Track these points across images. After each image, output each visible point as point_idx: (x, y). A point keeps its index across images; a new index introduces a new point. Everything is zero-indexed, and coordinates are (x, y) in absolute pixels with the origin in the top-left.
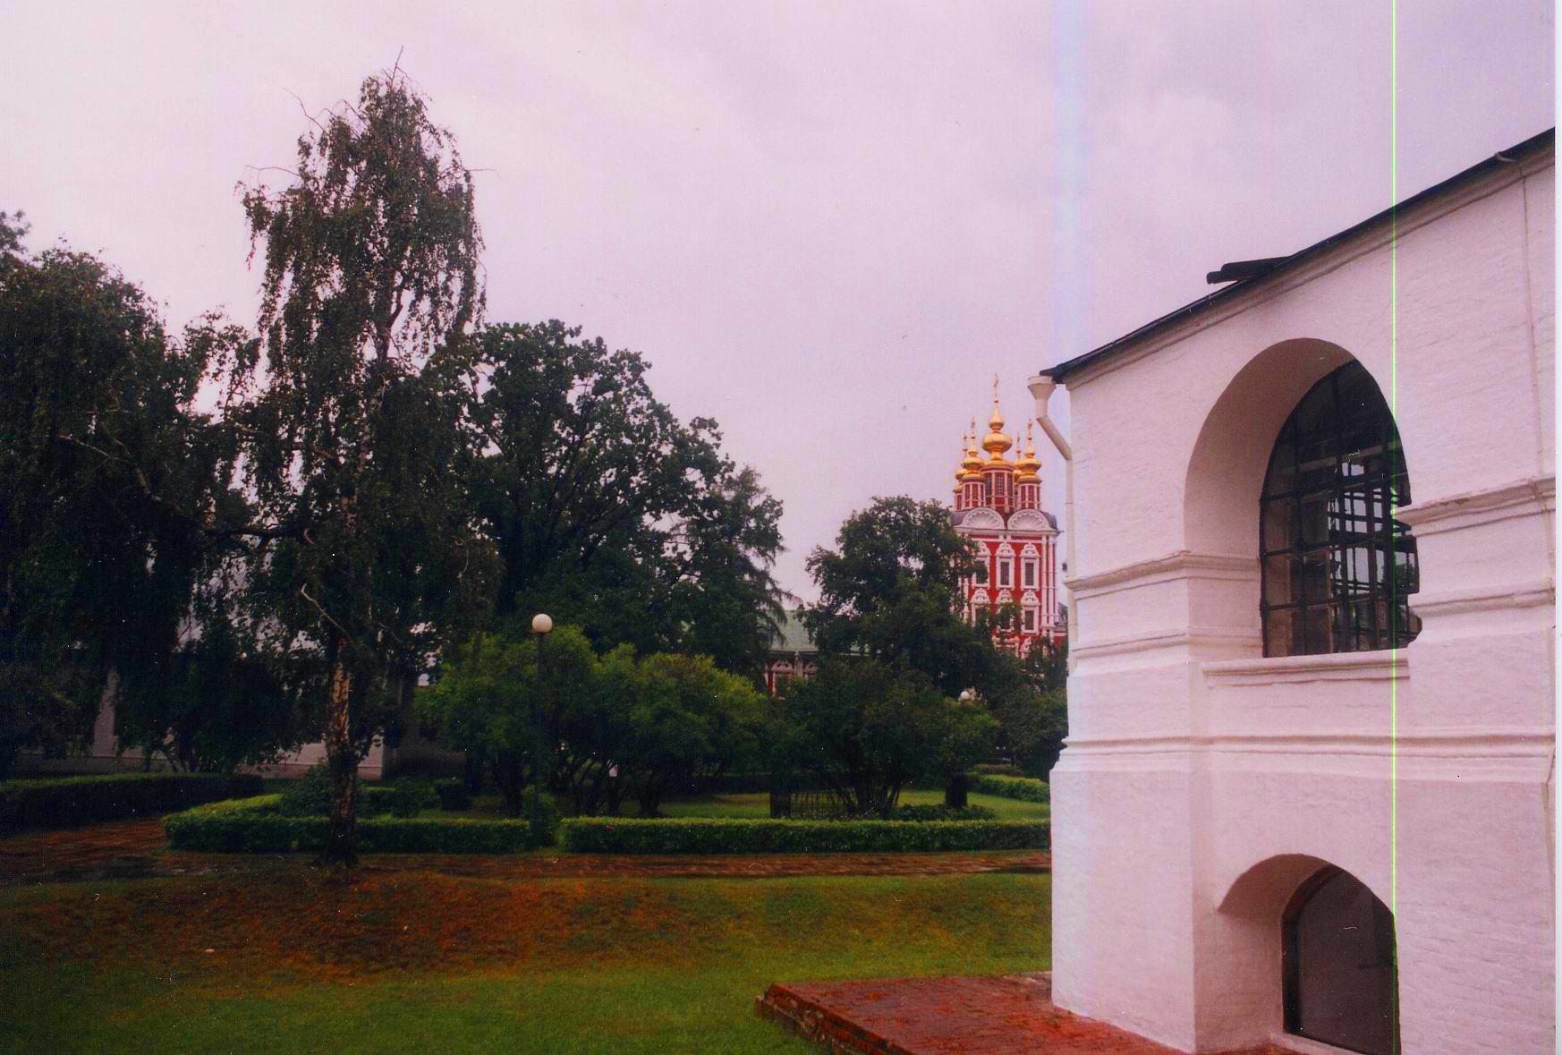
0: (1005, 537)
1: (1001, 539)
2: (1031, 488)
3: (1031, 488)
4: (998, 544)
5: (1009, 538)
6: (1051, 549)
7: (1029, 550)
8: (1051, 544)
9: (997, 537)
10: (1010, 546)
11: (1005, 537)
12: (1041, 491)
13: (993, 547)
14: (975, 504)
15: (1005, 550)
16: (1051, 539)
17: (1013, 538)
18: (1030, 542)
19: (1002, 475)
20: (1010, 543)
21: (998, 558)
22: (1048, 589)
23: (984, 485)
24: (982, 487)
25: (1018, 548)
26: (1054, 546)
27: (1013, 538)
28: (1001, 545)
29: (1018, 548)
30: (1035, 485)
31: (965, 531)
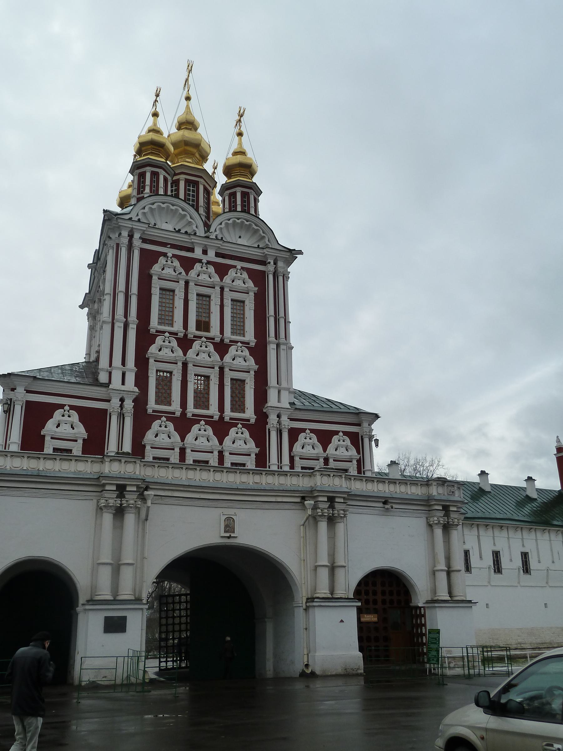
0: (205, 252)
1: (198, 253)
2: (245, 196)
5: (211, 256)
6: (281, 279)
8: (280, 270)
9: (192, 250)
10: (211, 269)
11: (205, 252)
16: (280, 264)
22: (278, 346)
23: (169, 178)
24: (166, 179)
26: (286, 277)
27: (218, 255)
31: (137, 225)
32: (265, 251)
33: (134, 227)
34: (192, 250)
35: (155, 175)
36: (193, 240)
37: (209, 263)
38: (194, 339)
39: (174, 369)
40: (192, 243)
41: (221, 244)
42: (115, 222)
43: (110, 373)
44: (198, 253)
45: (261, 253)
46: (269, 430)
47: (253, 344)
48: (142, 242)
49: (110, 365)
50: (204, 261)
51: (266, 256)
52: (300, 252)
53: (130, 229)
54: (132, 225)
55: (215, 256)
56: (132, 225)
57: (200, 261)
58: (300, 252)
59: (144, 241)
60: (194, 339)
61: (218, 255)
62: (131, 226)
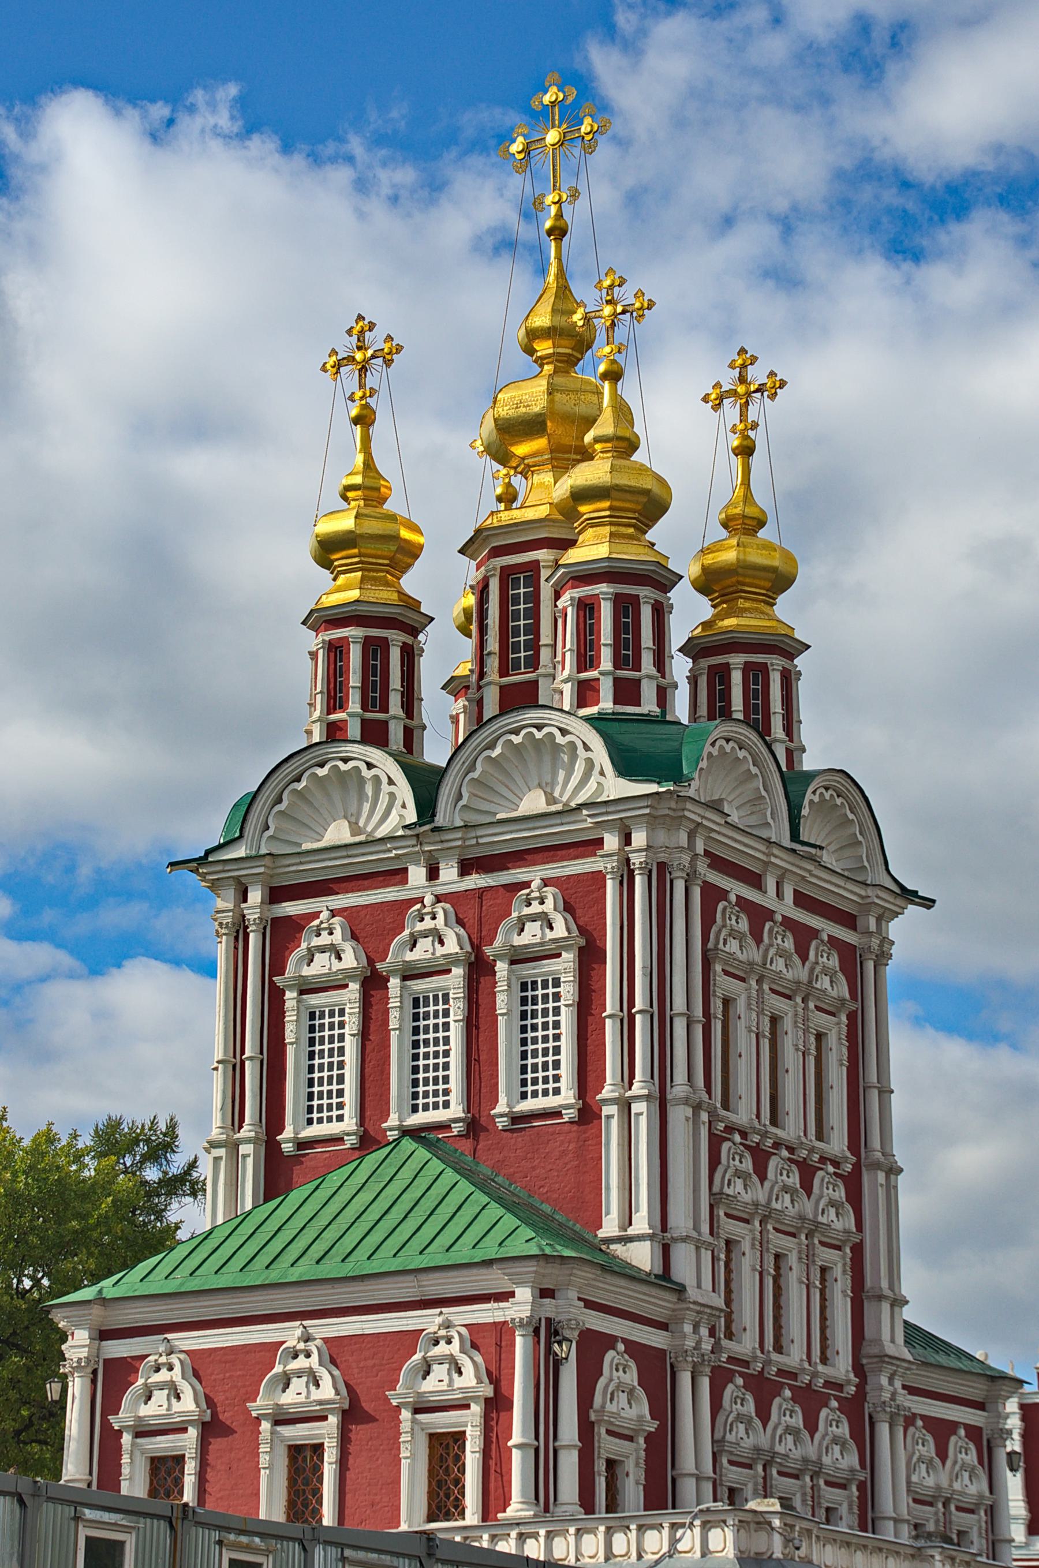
12: (804, 689)
21: (502, 968)
30: (776, 663)
32: (870, 892)
33: (705, 823)
36: (773, 860)
37: (788, 923)
38: (724, 1135)
39: (790, 1251)
41: (809, 871)
42: (673, 805)
43: (666, 1250)
45: (860, 896)
46: (871, 1417)
47: (849, 1168)
48: (709, 866)
49: (664, 1228)
50: (779, 918)
51: (867, 907)
52: (928, 903)
53: (692, 826)
54: (703, 817)
55: (794, 903)
56: (703, 817)
57: (769, 914)
58: (928, 903)
59: (718, 863)
60: (724, 1135)
62: (699, 820)
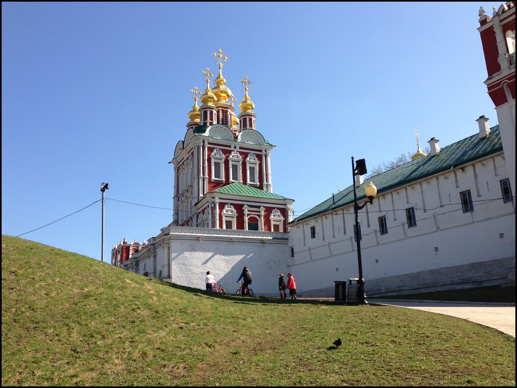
0: (235, 147)
1: (232, 148)
3: (250, 120)
4: (230, 152)
5: (238, 148)
7: (251, 160)
9: (230, 147)
11: (235, 147)
13: (227, 152)
14: (211, 124)
15: (235, 156)
17: (240, 148)
18: (252, 152)
19: (227, 111)
20: (239, 152)
25: (245, 155)
28: (233, 153)
29: (245, 155)
34: (230, 147)
35: (211, 113)
40: (230, 144)
44: (232, 148)
61: (240, 148)
